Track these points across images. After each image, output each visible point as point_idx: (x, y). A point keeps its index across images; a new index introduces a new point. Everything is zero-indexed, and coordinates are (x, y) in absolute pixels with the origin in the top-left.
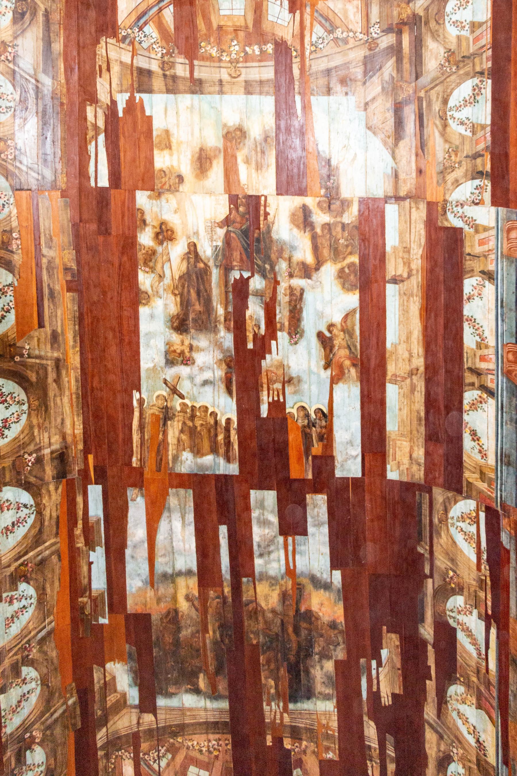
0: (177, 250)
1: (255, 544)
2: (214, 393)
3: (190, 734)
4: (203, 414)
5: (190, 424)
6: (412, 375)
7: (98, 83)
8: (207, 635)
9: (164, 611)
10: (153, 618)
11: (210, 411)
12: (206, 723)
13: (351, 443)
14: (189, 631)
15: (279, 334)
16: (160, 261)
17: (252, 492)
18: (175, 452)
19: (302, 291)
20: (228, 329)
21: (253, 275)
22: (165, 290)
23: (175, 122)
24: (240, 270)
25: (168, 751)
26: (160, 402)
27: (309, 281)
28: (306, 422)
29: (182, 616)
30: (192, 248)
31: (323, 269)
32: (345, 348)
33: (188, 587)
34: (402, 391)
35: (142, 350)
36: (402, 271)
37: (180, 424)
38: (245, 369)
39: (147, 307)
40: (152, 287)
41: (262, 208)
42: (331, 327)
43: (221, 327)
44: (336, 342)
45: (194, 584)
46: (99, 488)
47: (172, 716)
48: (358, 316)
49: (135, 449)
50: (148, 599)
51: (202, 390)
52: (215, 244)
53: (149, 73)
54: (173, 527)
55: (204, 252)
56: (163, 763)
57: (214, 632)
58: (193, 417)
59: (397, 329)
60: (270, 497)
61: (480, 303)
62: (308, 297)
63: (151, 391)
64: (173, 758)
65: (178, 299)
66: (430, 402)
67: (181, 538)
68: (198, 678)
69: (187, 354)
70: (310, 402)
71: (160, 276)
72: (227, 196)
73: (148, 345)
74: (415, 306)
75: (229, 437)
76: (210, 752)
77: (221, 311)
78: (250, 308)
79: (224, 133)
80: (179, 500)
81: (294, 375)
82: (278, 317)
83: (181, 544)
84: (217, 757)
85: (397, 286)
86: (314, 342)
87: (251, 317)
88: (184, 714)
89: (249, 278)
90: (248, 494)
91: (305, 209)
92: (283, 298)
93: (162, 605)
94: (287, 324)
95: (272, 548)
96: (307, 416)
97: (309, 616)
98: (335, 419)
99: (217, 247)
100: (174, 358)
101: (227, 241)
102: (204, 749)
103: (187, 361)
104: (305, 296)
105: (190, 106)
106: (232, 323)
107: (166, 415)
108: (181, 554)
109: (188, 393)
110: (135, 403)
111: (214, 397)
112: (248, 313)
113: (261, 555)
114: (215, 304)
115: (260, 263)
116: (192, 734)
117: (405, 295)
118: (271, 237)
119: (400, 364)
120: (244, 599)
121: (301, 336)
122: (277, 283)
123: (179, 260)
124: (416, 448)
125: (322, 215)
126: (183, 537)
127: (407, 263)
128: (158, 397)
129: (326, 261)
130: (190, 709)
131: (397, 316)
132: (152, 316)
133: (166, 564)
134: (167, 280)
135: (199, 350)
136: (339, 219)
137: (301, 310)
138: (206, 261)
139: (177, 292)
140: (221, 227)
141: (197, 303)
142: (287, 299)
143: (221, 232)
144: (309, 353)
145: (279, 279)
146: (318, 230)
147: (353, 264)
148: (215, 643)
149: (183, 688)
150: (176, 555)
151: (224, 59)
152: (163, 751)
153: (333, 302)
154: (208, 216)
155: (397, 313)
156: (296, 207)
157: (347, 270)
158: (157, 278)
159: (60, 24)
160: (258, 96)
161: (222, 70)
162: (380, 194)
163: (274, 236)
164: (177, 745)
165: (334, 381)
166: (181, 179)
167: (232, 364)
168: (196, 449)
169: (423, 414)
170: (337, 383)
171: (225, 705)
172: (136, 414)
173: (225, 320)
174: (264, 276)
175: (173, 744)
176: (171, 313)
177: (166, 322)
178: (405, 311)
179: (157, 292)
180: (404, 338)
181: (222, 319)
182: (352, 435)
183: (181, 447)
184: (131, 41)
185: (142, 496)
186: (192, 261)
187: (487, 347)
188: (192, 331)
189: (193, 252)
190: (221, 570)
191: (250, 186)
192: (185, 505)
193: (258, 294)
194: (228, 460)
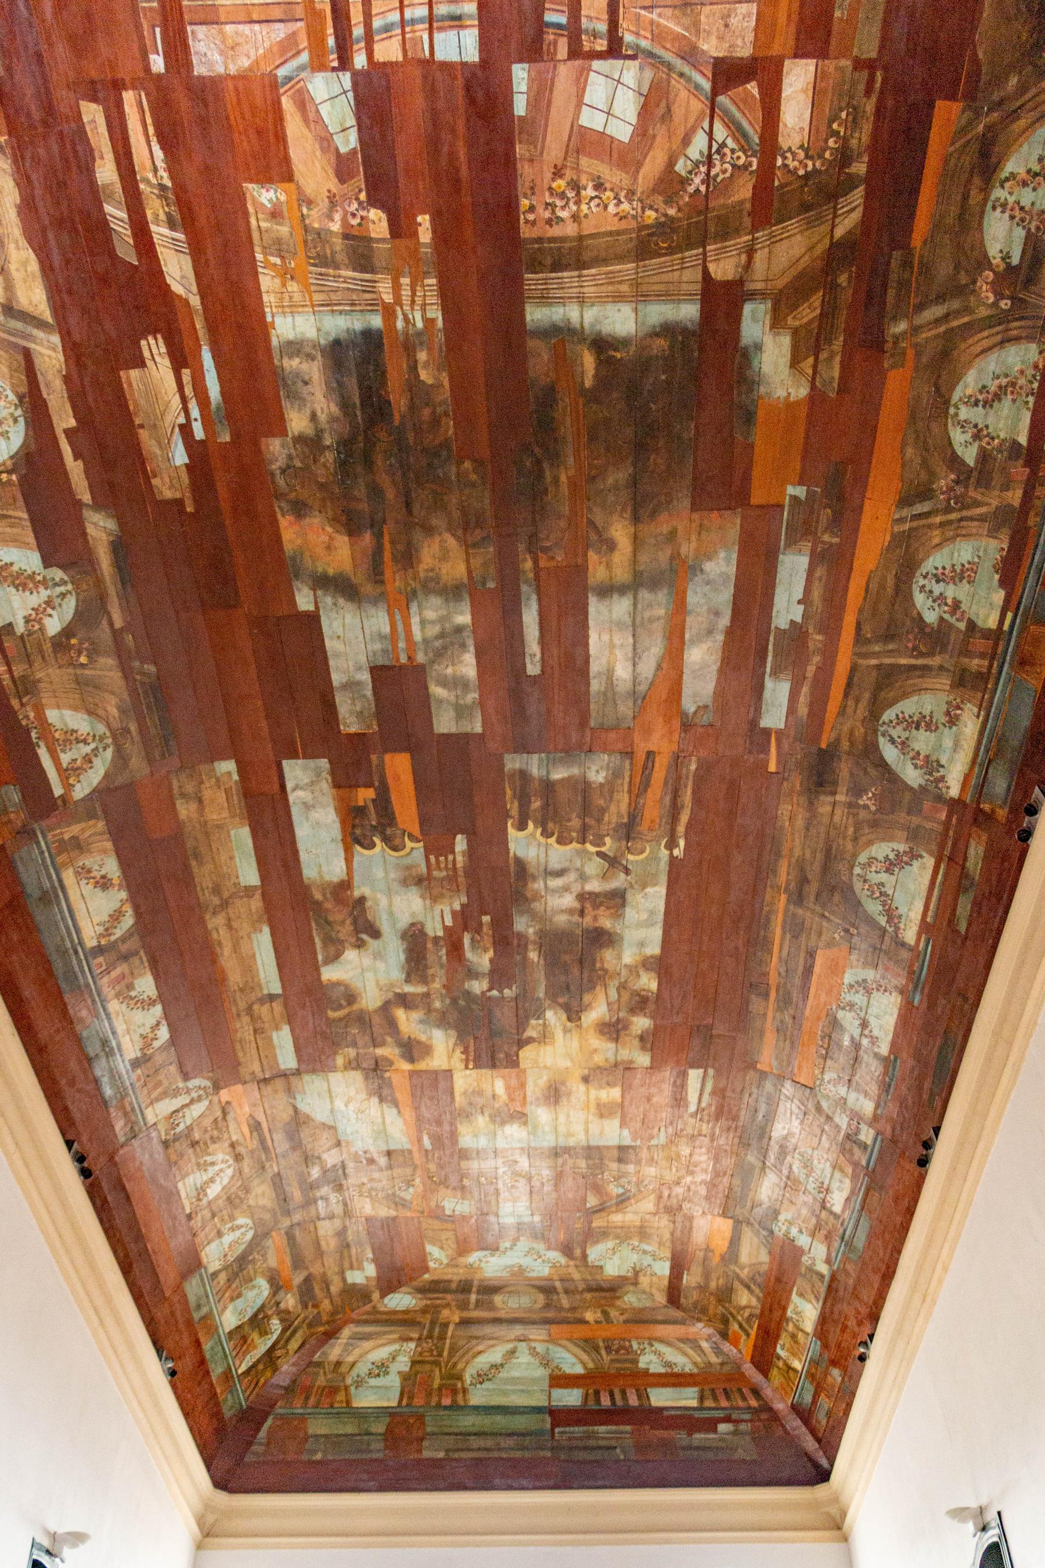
0: (598, 1011)
1: (472, 649)
3: (625, 232)
6: (221, 905)
8: (572, 472)
9: (663, 516)
10: (687, 503)
11: (554, 838)
12: (581, 265)
13: (307, 807)
14: (610, 481)
15: (440, 933)
17: (478, 729)
18: (619, 782)
19: (408, 980)
25: (684, 182)
27: (398, 991)
28: (388, 832)
29: (624, 510)
31: (379, 1004)
33: (609, 566)
34: (233, 880)
36: (264, 1011)
37: (606, 819)
38: (495, 893)
40: (638, 976)
42: (360, 945)
44: (348, 927)
45: (595, 569)
47: (665, 278)
48: (320, 958)
50: (693, 538)
51: (567, 864)
54: (631, 668)
56: (699, 144)
57: (556, 481)
58: (584, 830)
60: (444, 723)
61: (141, 1031)
63: (654, 858)
64: (671, 163)
66: (186, 880)
67: (617, 652)
68: (596, 376)
73: (652, 913)
74: (235, 978)
75: (521, 806)
76: (576, 186)
77: (533, 955)
81: (414, 889)
82: (444, 951)
83: (617, 641)
84: (558, 173)
85: (265, 992)
86: (385, 927)
87: (486, 950)
88: (636, 284)
91: (411, 1060)
93: (665, 529)
94: (429, 945)
95: (438, 644)
96: (386, 840)
97: (350, 523)
98: (339, 837)
99: (538, 1018)
102: (590, 192)
104: (404, 976)
107: (628, 831)
108: (620, 625)
109: (590, 859)
110: (682, 843)
112: (491, 953)
113: (459, 630)
114: (542, 962)
116: (618, 233)
117: (251, 984)
120: (492, 549)
124: (194, 816)
126: (611, 652)
127: (254, 1018)
128: (642, 852)
129: (375, 1011)
130: (618, 298)
133: (650, 606)
135: (570, 911)
137: (408, 960)
143: (530, 1033)
144: (391, 914)
147: (335, 1010)
148: (555, 457)
149: (633, 349)
150: (628, 620)
152: (697, 180)
154: (548, 1048)
158: (630, 985)
162: (307, 1078)
164: (659, 200)
165: (346, 885)
169: (194, 863)
171: (535, 315)
172: (681, 829)
175: (668, 202)
177: (622, 938)
178: (249, 966)
182: (307, 818)
187: (117, 996)
189: (573, 1013)
190: (540, 600)
194: (523, 774)
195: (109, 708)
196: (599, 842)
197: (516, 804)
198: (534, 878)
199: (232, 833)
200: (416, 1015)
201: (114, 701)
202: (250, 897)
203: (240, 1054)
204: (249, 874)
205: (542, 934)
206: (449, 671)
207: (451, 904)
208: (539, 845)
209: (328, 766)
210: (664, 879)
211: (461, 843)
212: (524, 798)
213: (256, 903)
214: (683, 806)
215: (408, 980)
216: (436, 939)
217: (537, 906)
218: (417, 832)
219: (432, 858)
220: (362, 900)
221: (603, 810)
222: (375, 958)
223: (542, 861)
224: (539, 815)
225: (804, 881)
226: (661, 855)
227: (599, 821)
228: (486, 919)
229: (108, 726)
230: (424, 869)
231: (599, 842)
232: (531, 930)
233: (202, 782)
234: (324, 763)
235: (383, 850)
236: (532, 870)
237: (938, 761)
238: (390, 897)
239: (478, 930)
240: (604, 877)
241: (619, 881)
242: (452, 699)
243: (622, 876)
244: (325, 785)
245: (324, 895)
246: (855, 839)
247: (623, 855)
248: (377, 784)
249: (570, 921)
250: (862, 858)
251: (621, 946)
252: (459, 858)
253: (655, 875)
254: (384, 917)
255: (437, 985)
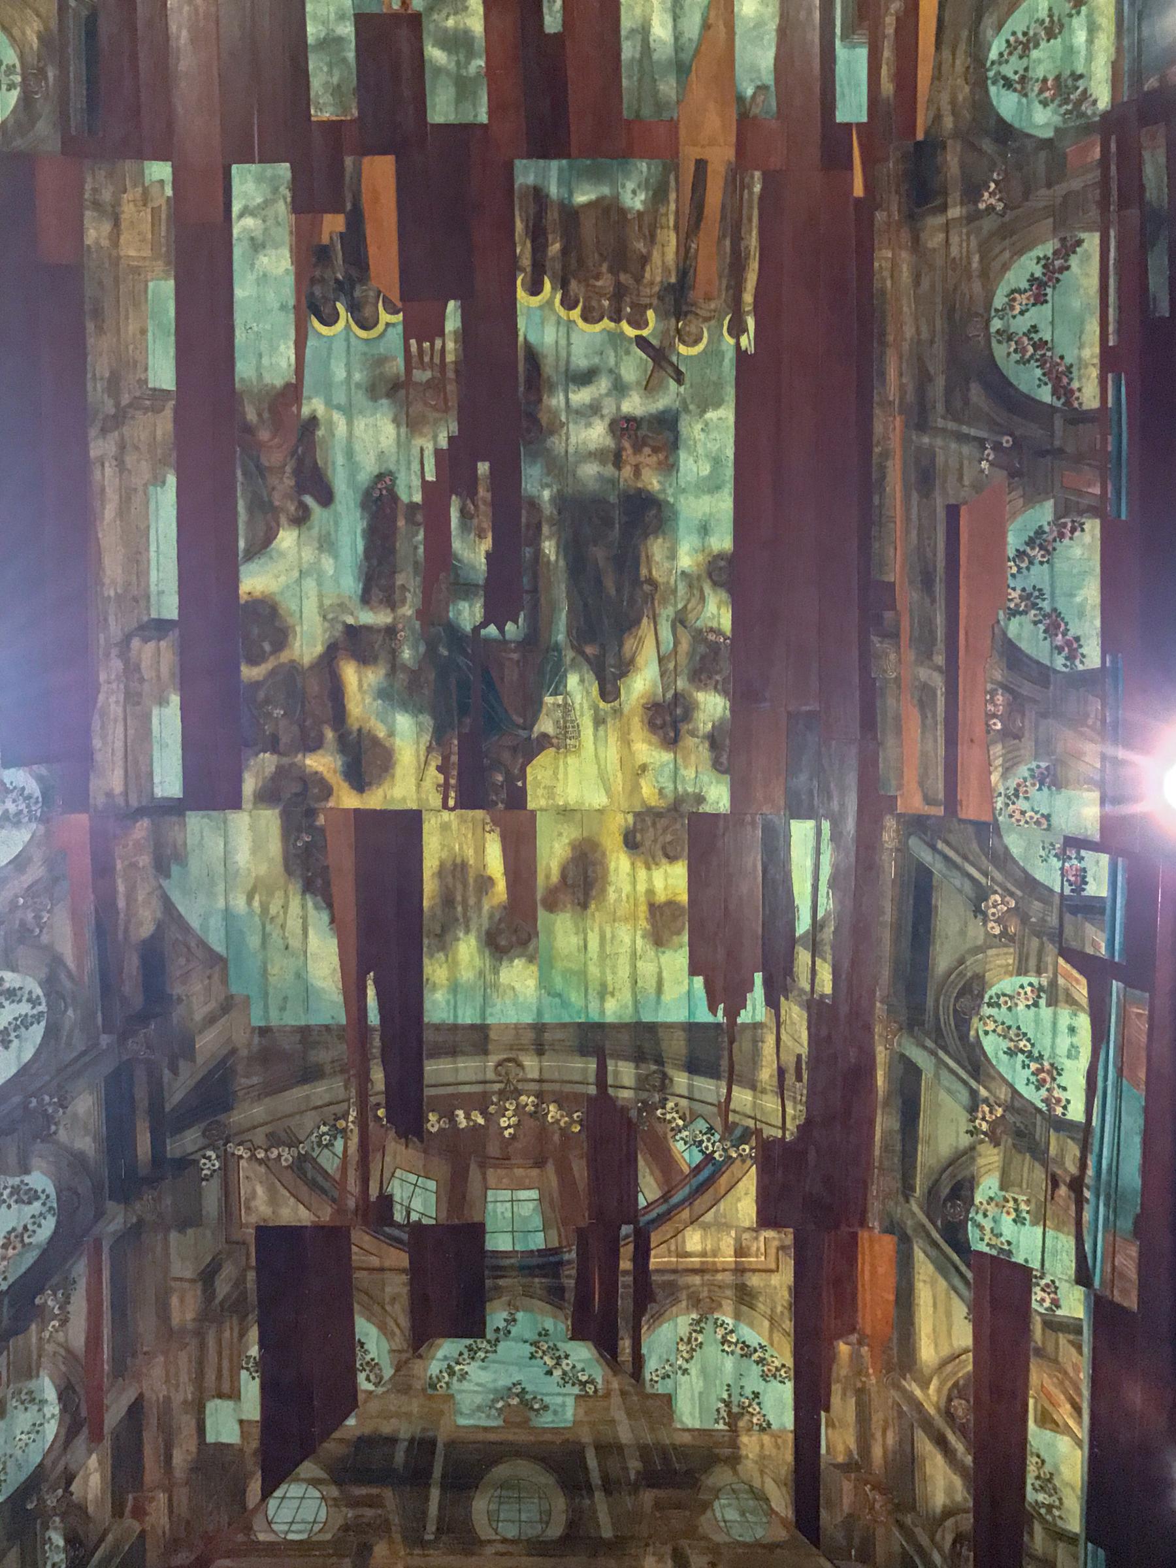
2: (569, 354)
4: (594, 303)
5: (623, 277)
7: (806, 1044)
15: (417, 498)
16: (682, 659)
17: (483, 118)
19: (366, 599)
20: (534, 505)
21: (476, 629)
22: (674, 591)
23: (639, 964)
24: (505, 642)
26: (693, 329)
27: (350, 621)
28: (357, 294)
30: (609, 687)
31: (319, 649)
32: (270, 469)
35: (730, 452)
39: (715, 552)
41: (453, 781)
42: (301, 519)
43: (548, 509)
44: (289, 482)
46: (842, 115)
48: (242, 544)
49: (756, 213)
52: (560, 699)
53: (693, 1067)
54: (670, 26)
55: (582, 681)
58: (619, 294)
59: (152, 518)
60: (442, 108)
62: (350, 585)
65: (644, 572)
69: (626, 444)
70: (347, 340)
71: (683, 623)
72: (531, 805)
75: (535, 251)
77: (549, 547)
78: (483, 554)
79: (534, 941)
80: (655, 92)
81: (384, 401)
82: (421, 536)
85: (154, 615)
87: (481, 536)
89: (484, 625)
90: (491, 113)
91: (358, 778)
92: (408, 580)
94: (401, 523)
98: (292, 302)
99: (555, 693)
100: (658, 435)
101: (533, 708)
103: (624, 427)
105: (608, 997)
106: (524, 520)
107: (678, 300)
109: (628, 353)
111: (569, 344)
112: (486, 545)
114: (562, 563)
115: (461, 660)
117: (137, 594)
118: (435, 718)
119: (144, 436)
121: (367, 493)
122: (420, 614)
123: (640, 660)
125: (321, 769)
129: (313, 667)
131: (153, 548)
132: (704, 529)
134: (667, 613)
136: (285, 760)
138: (580, 659)
139: (647, 588)
140: (545, 736)
141: (601, 564)
142: (400, 580)
143: (546, 726)
144: (350, 454)
145: (417, 625)
146: (329, 735)
147: (254, 662)
151: (532, 1099)
153: (296, 574)
155: (153, 555)
156: (379, 785)
157: (267, 647)
159: (881, 1168)
160: (460, 1021)
161: (536, 1075)
163: (427, 720)
165: (293, 392)
166: (631, 842)
167: (524, 424)
168: (614, 217)
170: (288, 385)
173: (539, 527)
174: (453, 630)
176: (660, 540)
178: (137, 559)
179: (690, 586)
180: (137, 500)
181: (546, 530)
183: (647, 220)
184: (731, 1134)
185: (740, 99)
186: (611, 660)
188: (613, 499)
189: (609, 678)
191: (480, 830)
192: (640, 80)
193: (465, 589)
194: (538, 194)
195: (29, 32)
196: (638, 322)
197: (529, 245)
198: (552, 388)
199: (151, 285)
200: (374, 676)
201: (37, 25)
202: (157, 410)
203: (97, 743)
204: (162, 371)
205: (560, 500)
206: (451, 23)
207: (435, 437)
208: (559, 323)
209: (289, 175)
210: (730, 393)
211: (453, 320)
212: (538, 235)
213: (164, 424)
214: (747, 257)
215: (366, 599)
216: (413, 506)
217: (556, 443)
218: (395, 296)
219: (413, 342)
220: (313, 421)
221: (645, 260)
222: (321, 548)
223: (563, 354)
224: (558, 266)
225: (924, 379)
226: (724, 348)
227: (638, 279)
228: (483, 468)
229: (22, 57)
230: (398, 365)
231: (639, 323)
232: (546, 494)
233: (125, 192)
234: (284, 170)
235: (348, 326)
236: (548, 369)
237: (1073, 74)
238: (350, 423)
239: (470, 491)
240: (650, 387)
241: (669, 397)
242: (452, 66)
243: (672, 384)
244: (282, 208)
245: (260, 415)
246: (985, 274)
247: (672, 346)
248: (349, 206)
249: (600, 477)
250: (999, 301)
251: (675, 530)
252: (450, 345)
253: (719, 385)
254: (340, 460)
255: (407, 611)
